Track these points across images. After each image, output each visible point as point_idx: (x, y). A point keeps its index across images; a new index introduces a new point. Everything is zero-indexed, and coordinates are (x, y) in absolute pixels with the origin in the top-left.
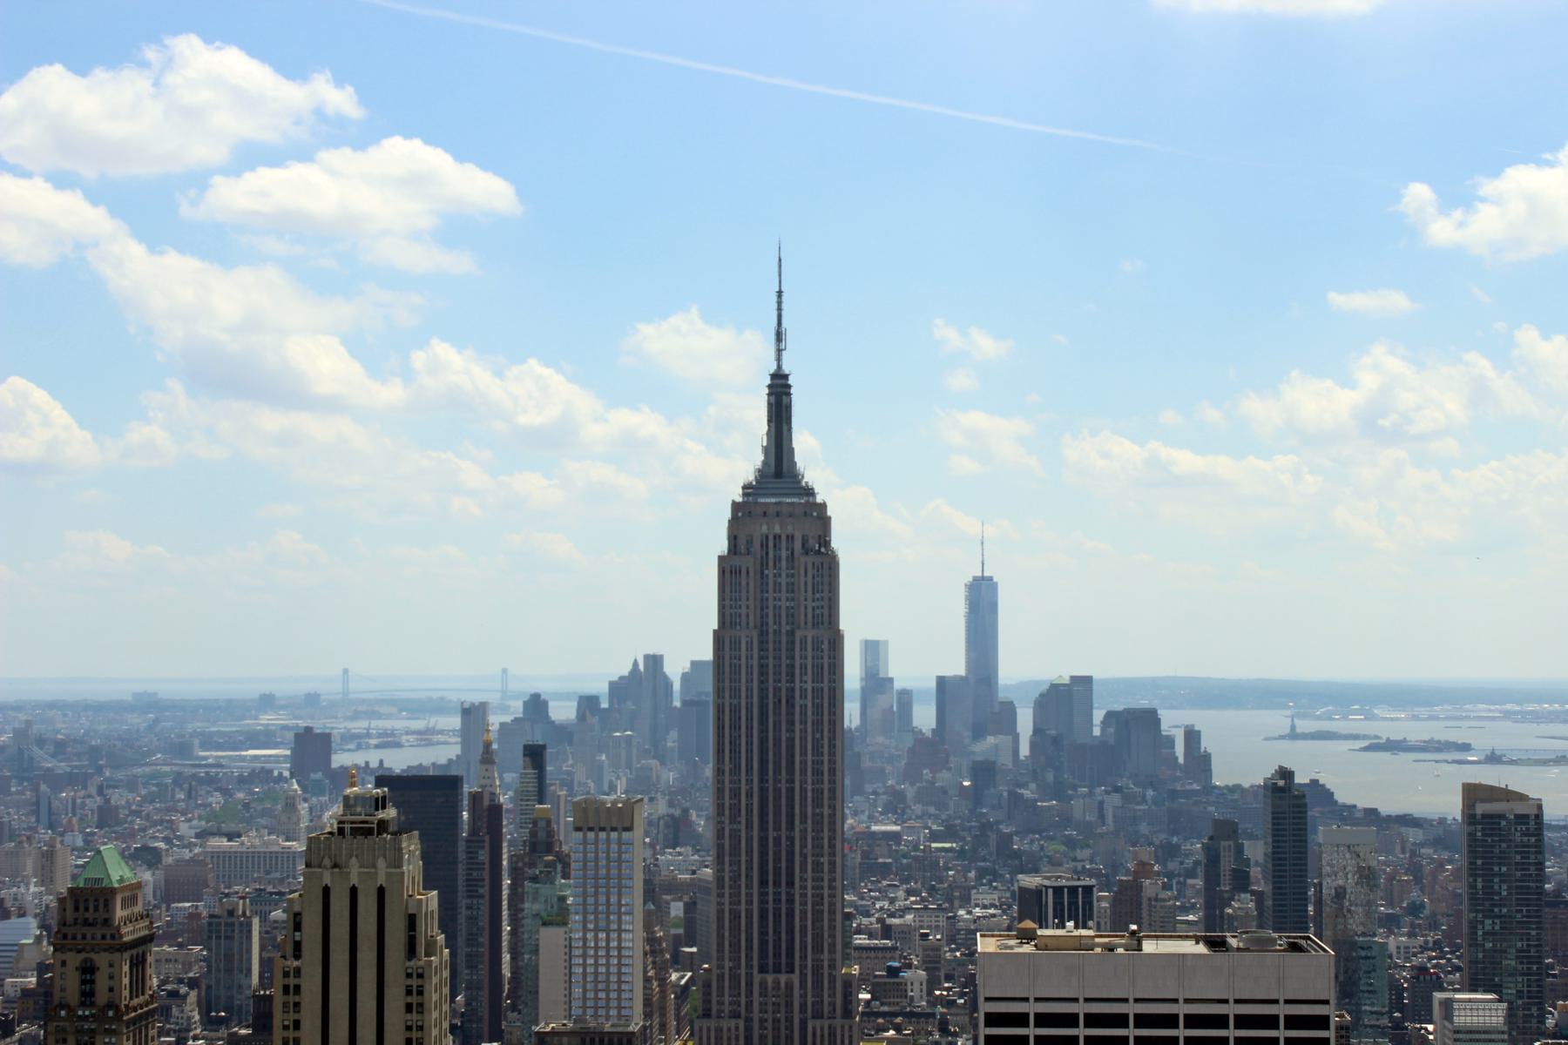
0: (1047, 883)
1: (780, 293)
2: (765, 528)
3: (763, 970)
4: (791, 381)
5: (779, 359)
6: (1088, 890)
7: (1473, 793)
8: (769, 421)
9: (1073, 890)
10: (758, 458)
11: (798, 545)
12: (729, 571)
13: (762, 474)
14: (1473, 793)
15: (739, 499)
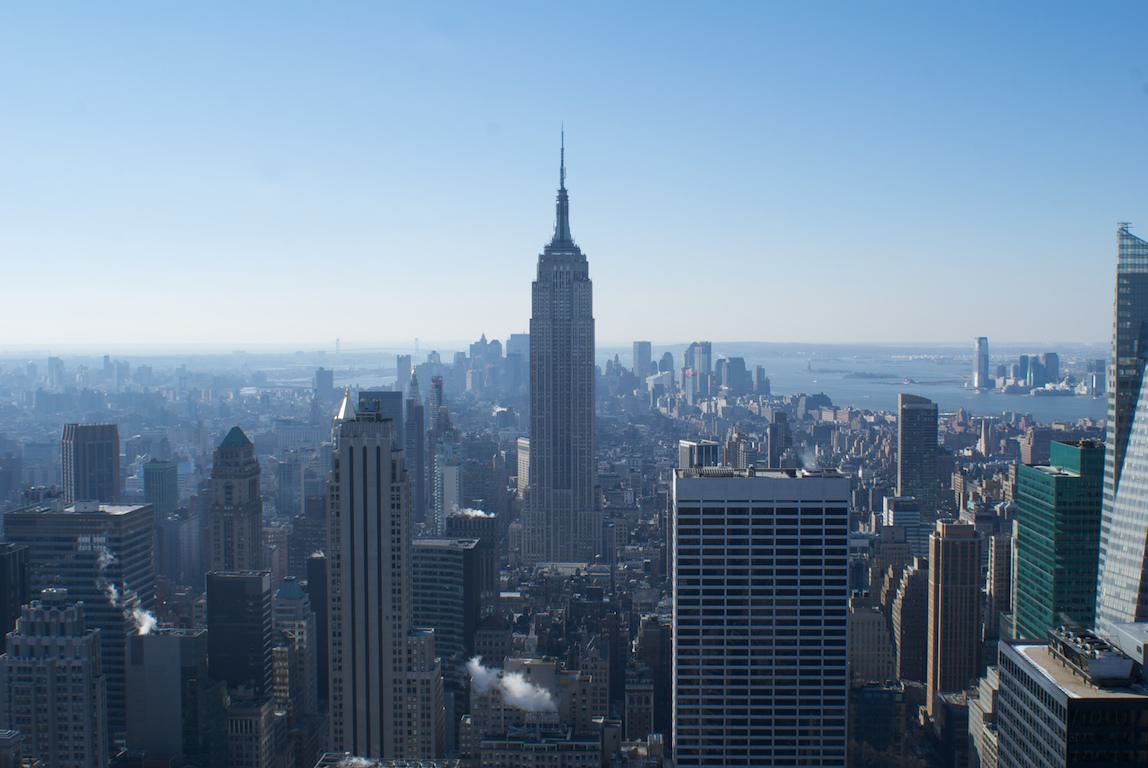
0: (695, 444)
1: (562, 149)
2: (555, 268)
3: (555, 487)
4: (568, 193)
5: (562, 184)
6: (715, 447)
7: (906, 398)
8: (558, 214)
9: (708, 447)
10: (548, 234)
11: (572, 277)
12: (536, 287)
13: (555, 241)
14: (906, 398)
15: (542, 253)
